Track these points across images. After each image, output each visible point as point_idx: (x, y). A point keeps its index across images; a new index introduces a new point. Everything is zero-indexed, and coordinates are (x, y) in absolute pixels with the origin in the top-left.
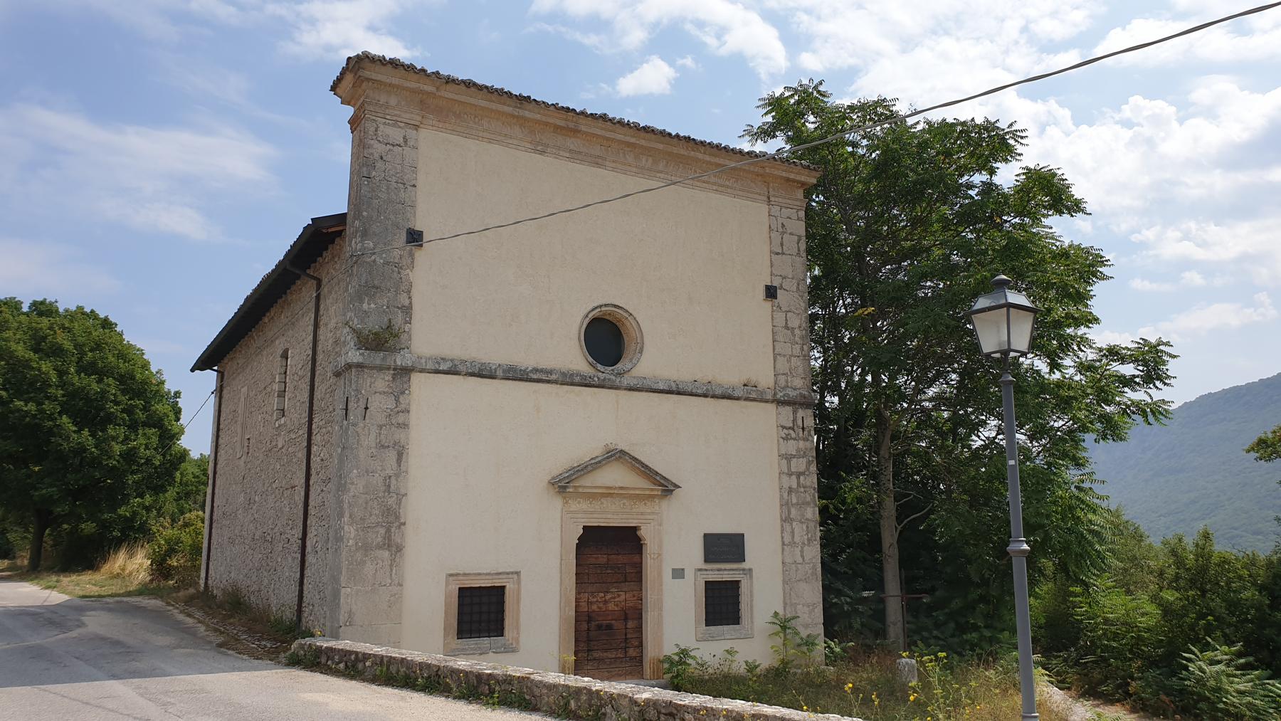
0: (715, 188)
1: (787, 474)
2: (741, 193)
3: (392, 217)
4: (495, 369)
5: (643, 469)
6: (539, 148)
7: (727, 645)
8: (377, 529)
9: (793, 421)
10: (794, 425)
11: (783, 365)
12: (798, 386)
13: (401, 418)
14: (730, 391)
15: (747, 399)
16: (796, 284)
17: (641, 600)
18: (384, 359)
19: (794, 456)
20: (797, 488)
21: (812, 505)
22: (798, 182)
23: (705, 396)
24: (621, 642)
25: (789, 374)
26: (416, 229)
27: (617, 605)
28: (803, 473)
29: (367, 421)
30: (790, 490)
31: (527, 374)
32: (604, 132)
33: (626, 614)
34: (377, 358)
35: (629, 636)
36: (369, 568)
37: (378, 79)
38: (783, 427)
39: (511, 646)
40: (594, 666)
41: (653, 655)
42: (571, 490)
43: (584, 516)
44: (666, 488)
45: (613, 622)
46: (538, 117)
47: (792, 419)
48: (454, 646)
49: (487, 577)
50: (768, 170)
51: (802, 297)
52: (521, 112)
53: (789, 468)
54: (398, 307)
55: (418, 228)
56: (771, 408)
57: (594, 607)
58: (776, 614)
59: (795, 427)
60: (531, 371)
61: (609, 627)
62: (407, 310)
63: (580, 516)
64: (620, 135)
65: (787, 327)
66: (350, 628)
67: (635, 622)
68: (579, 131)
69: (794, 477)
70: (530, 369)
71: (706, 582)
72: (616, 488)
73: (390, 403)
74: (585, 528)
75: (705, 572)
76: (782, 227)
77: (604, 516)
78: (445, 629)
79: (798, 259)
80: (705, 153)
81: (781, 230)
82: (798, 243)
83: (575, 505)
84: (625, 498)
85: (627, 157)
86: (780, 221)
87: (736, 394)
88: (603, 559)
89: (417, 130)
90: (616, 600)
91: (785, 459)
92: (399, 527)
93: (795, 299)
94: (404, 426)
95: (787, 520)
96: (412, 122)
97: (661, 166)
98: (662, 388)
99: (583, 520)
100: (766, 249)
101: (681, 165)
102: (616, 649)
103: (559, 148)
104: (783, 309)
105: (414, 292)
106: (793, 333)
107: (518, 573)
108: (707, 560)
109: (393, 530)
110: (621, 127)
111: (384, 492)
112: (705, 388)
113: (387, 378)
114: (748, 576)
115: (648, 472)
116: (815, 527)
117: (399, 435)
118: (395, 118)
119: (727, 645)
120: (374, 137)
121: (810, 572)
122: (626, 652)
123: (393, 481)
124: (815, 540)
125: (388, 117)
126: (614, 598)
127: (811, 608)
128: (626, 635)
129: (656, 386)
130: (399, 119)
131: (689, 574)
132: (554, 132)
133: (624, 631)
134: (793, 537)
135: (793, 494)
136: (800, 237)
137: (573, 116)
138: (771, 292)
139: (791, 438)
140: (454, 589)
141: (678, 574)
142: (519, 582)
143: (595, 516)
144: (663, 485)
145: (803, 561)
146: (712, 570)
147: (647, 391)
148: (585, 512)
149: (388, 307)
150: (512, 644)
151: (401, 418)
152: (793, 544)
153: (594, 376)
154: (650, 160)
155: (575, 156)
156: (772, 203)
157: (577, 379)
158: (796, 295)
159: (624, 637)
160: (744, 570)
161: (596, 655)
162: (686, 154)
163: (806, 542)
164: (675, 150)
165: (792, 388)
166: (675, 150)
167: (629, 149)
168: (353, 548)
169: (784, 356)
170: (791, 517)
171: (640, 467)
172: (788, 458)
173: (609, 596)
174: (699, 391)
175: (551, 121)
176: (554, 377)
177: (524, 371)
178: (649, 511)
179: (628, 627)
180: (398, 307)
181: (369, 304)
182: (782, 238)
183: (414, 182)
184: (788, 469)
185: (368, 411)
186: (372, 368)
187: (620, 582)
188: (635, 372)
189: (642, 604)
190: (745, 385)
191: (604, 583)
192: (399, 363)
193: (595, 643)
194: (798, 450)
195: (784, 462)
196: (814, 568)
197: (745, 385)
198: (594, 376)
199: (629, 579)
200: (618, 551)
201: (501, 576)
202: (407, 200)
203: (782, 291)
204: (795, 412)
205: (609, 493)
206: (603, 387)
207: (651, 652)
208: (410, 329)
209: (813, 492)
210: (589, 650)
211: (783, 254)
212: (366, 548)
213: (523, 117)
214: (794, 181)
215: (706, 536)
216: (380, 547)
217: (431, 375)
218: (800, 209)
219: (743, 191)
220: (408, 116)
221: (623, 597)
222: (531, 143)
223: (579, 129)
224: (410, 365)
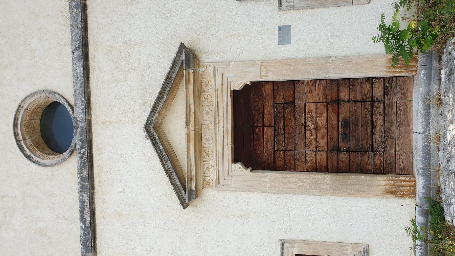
5: (165, 97)
17: (316, 81)
24: (365, 107)
27: (321, 114)
31: (87, 227)
35: (358, 97)
39: (362, 254)
40: (392, 143)
42: (193, 185)
45: (341, 118)
57: (323, 143)
60: (84, 223)
61: (346, 123)
63: (221, 169)
67: (342, 88)
70: (81, 224)
74: (235, 161)
77: (221, 139)
83: (211, 174)
84: (200, 113)
88: (268, 133)
90: (315, 115)
98: (82, 69)
102: (373, 113)
112: (75, 11)
115: (168, 89)
122: (378, 101)
128: (356, 101)
129: (81, 77)
142: (293, 241)
148: (217, 163)
150: (360, 252)
153: (80, 153)
157: (85, 173)
159: (359, 103)
161: (378, 140)
171: (164, 100)
173: (310, 125)
176: (86, 199)
187: (295, 110)
189: (320, 80)
191: (294, 132)
193: (364, 142)
198: (80, 153)
199: (291, 99)
200: (259, 114)
210: (373, 151)
221: (311, 106)
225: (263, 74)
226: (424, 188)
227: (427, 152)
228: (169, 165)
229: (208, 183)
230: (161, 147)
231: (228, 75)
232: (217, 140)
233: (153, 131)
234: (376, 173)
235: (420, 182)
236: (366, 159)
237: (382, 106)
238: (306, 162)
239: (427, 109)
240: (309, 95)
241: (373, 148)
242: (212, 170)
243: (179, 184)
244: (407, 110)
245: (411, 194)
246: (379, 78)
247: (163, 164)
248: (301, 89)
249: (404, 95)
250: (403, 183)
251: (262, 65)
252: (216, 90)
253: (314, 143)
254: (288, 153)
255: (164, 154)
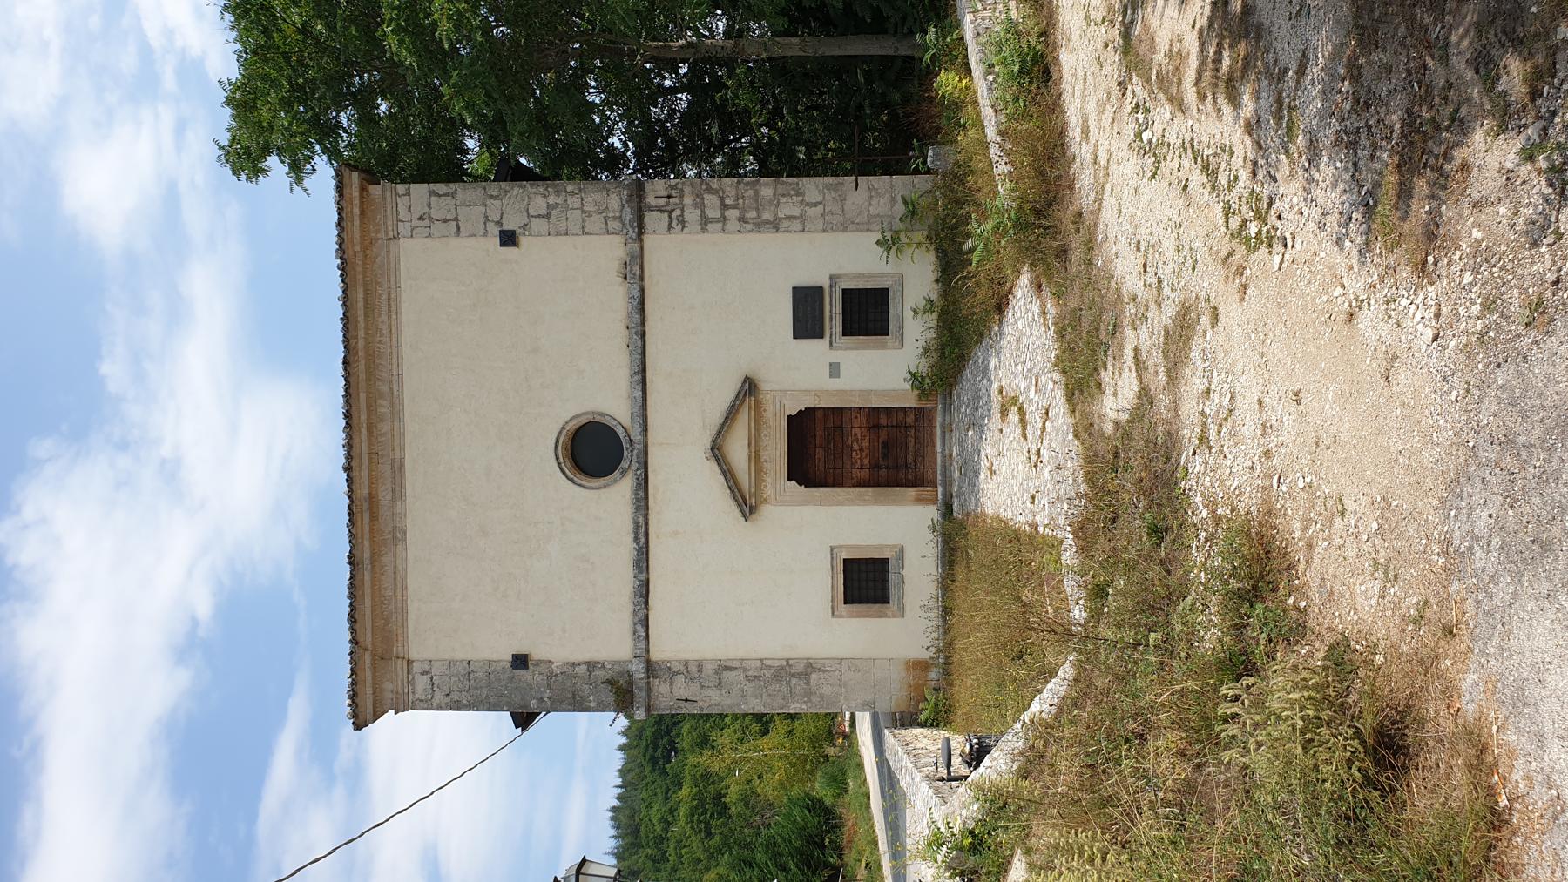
0: (394, 317)
1: (724, 224)
2: (393, 279)
3: (504, 683)
4: (639, 581)
6: (399, 535)
7: (909, 314)
8: (792, 685)
9: (661, 211)
10: (666, 211)
11: (595, 222)
12: (618, 201)
13: (693, 669)
14: (635, 303)
15: (642, 278)
16: (492, 200)
17: (860, 408)
18: (640, 689)
19: (703, 212)
20: (739, 209)
21: (758, 187)
22: (361, 197)
23: (643, 335)
25: (604, 214)
26: (511, 660)
27: (864, 436)
28: (722, 199)
29: (697, 699)
30: (742, 219)
31: (641, 548)
32: (364, 467)
33: (874, 426)
34: (640, 695)
35: (894, 423)
36: (826, 690)
37: (371, 707)
38: (670, 227)
41: (913, 401)
42: (753, 501)
43: (778, 482)
44: (749, 387)
45: (881, 441)
46: (366, 543)
47: (659, 212)
48: (896, 607)
49: (835, 578)
50: (357, 248)
51: (506, 192)
52: (367, 562)
53: (716, 220)
54: (590, 675)
55: (510, 659)
56: (649, 240)
57: (866, 461)
58: (878, 243)
59: (669, 208)
60: (638, 544)
61: (885, 445)
62: (591, 666)
64: (363, 447)
65: (548, 216)
66: (876, 704)
68: (370, 494)
69: (728, 213)
70: (635, 545)
71: (843, 335)
72: (750, 452)
73: (680, 679)
74: (790, 479)
75: (834, 337)
76: (424, 219)
77: (778, 459)
78: (881, 617)
79: (460, 195)
80: (356, 337)
81: (427, 221)
82: (440, 196)
83: (769, 492)
85: (383, 431)
86: (416, 223)
87: (637, 294)
88: (820, 453)
89: (413, 661)
91: (706, 225)
92: (791, 666)
93: (511, 203)
94: (700, 666)
95: (775, 225)
96: (405, 667)
97: (384, 388)
98: (641, 393)
99: (782, 483)
100: (454, 242)
101: (377, 361)
103: (394, 514)
104: (526, 221)
105: (572, 659)
106: (556, 206)
107: (832, 549)
108: (821, 336)
109: (793, 671)
110: (354, 449)
111: (760, 680)
112: (635, 337)
113: (657, 683)
114: (838, 280)
116: (783, 183)
117: (709, 669)
118: (406, 685)
119: (909, 314)
120: (430, 702)
121: (833, 194)
123: (750, 673)
124: (798, 184)
125: (406, 691)
126: (857, 440)
127: (873, 194)
128: (892, 426)
129: (640, 400)
130: (405, 680)
131: (836, 356)
132: (378, 520)
133: (890, 428)
134: (794, 217)
135: (746, 215)
136: (432, 193)
137: (356, 506)
138: (508, 239)
139: (682, 215)
140: (844, 609)
141: (835, 370)
142: (841, 547)
143: (778, 468)
144: (745, 395)
145: (820, 203)
146: (831, 329)
147: (646, 410)
148: (774, 481)
149: (591, 684)
150: (896, 552)
151: (693, 669)
152: (802, 218)
153: (636, 474)
154: (380, 402)
155: (398, 494)
156: (396, 234)
157: (641, 494)
158: (505, 200)
160: (831, 286)
161: (910, 460)
162: (364, 362)
163: (800, 198)
164: (362, 376)
165: (621, 211)
166: (362, 376)
167: (375, 430)
168: (809, 704)
169: (584, 221)
170: (772, 220)
172: (705, 222)
173: (856, 447)
174: (639, 344)
175: (367, 528)
176: (641, 519)
177: (638, 551)
178: (772, 407)
179: (885, 424)
180: (590, 675)
181: (590, 701)
182: (437, 220)
183: (465, 664)
184: (718, 222)
185: (689, 698)
186: (649, 697)
188: (626, 422)
190: (626, 278)
192: (643, 675)
193: (900, 461)
194: (695, 206)
195: (710, 227)
196: (828, 187)
197: (626, 278)
198: (636, 474)
201: (835, 565)
202: (484, 670)
203: (504, 221)
204: (651, 209)
205: (756, 457)
206: (646, 463)
207: (911, 401)
208: (609, 662)
209: (742, 185)
210: (907, 468)
211: (456, 219)
212: (809, 694)
213: (372, 557)
214: (362, 203)
215: (795, 290)
216: (808, 683)
217: (650, 640)
218: (396, 191)
219: (389, 277)
220: (400, 673)
221: (857, 430)
222: (396, 545)
223: (367, 496)
224: (643, 665)
225: (817, 402)
226: (942, 495)
227: (944, 466)
228: (732, 483)
229: (765, 500)
230: (724, 467)
231: (786, 402)
232: (774, 460)
233: (717, 452)
234: (909, 486)
235: (940, 489)
236: (901, 475)
237: (913, 431)
238: (852, 478)
239: (943, 433)
240: (855, 420)
241: (906, 466)
242: (769, 486)
243: (741, 500)
244: (932, 435)
245: (934, 501)
246: (910, 408)
247: (727, 482)
248: (849, 415)
249: (930, 421)
250: (929, 493)
251: (815, 395)
252: (775, 415)
253: (859, 461)
254: (838, 471)
255: (727, 473)
